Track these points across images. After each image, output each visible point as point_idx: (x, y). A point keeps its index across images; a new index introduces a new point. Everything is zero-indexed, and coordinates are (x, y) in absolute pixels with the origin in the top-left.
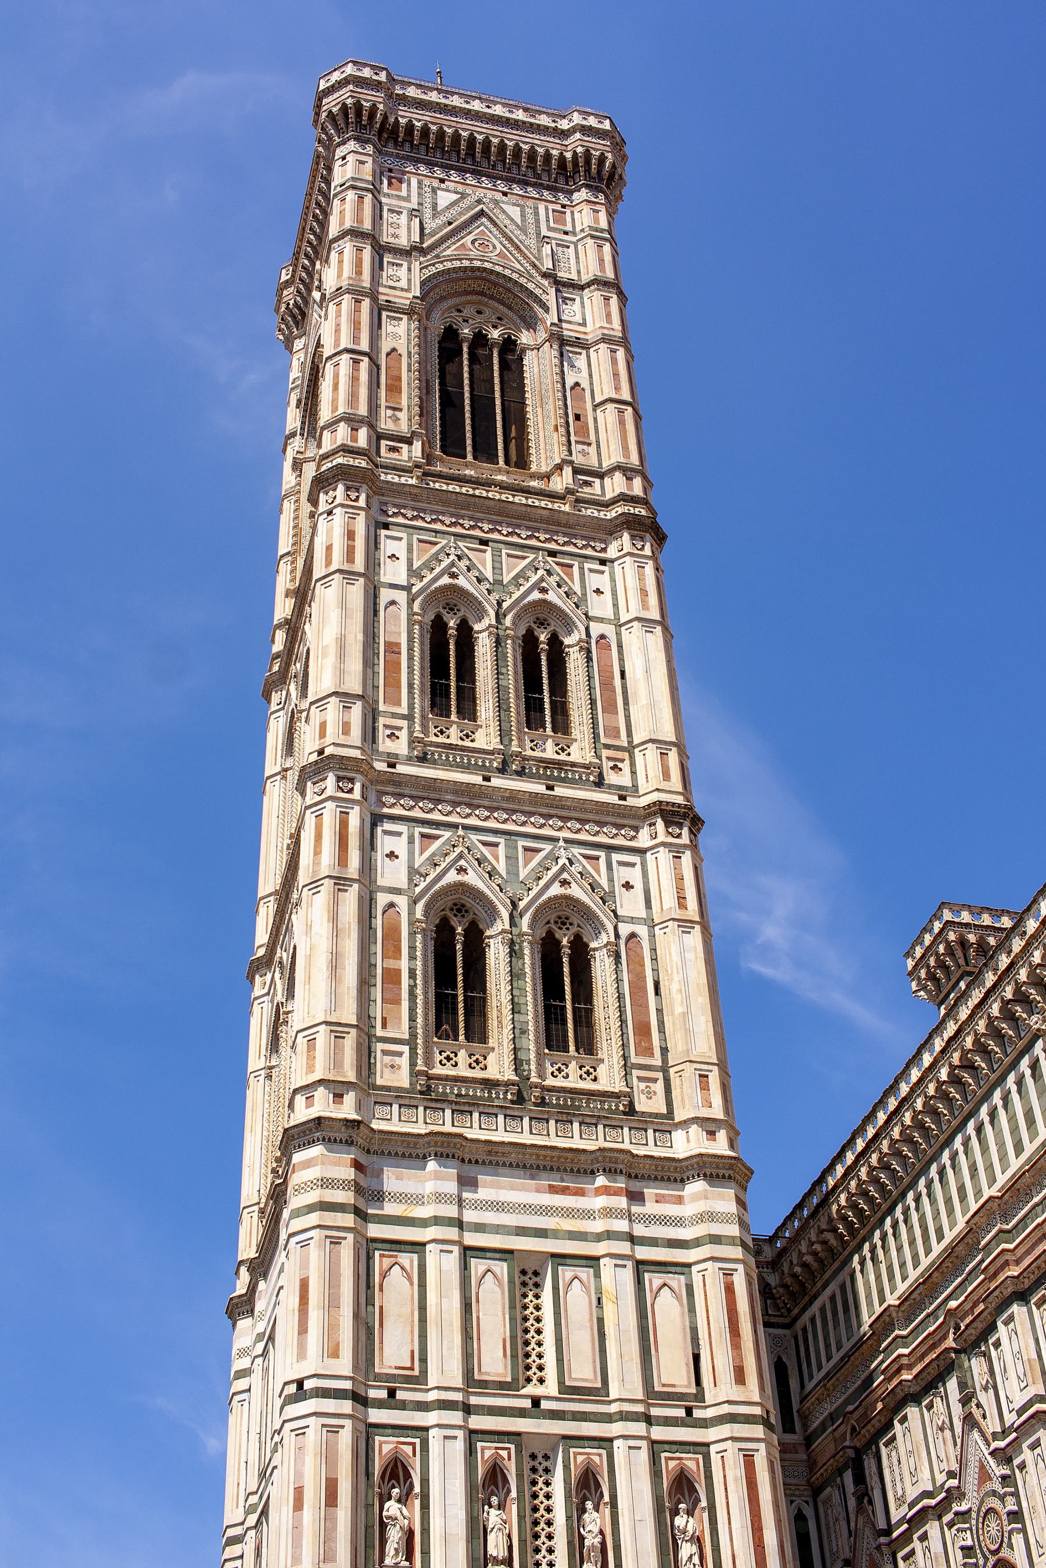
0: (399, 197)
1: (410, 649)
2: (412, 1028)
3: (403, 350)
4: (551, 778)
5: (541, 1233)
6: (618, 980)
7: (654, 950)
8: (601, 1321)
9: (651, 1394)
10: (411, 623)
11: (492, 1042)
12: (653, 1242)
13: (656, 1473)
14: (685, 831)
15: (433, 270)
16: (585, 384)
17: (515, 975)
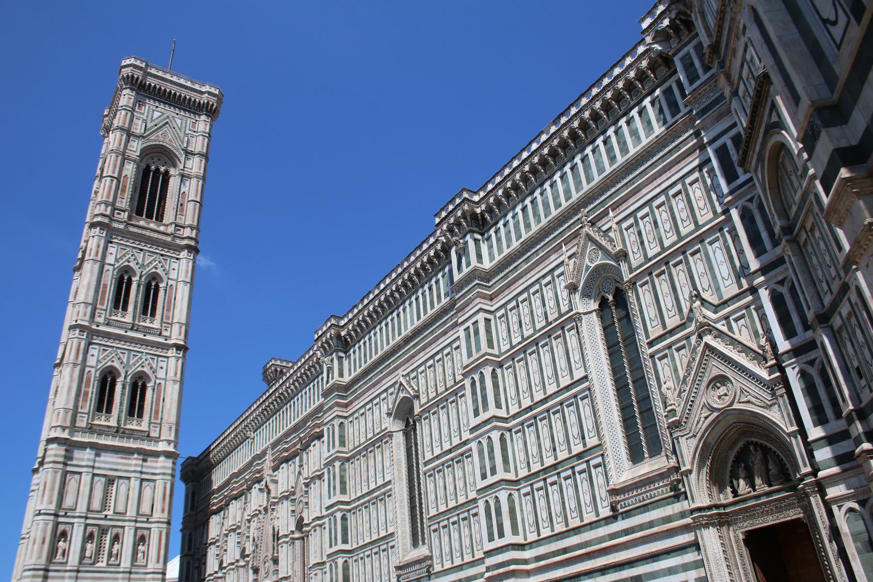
0: (141, 113)
1: (111, 286)
2: (90, 409)
3: (129, 176)
4: (146, 332)
5: (116, 470)
6: (153, 397)
7: (165, 388)
8: (128, 495)
9: (138, 513)
10: (112, 278)
11: (113, 414)
12: (147, 473)
13: (135, 535)
14: (182, 352)
15: (146, 145)
16: (187, 193)
17: (123, 394)
